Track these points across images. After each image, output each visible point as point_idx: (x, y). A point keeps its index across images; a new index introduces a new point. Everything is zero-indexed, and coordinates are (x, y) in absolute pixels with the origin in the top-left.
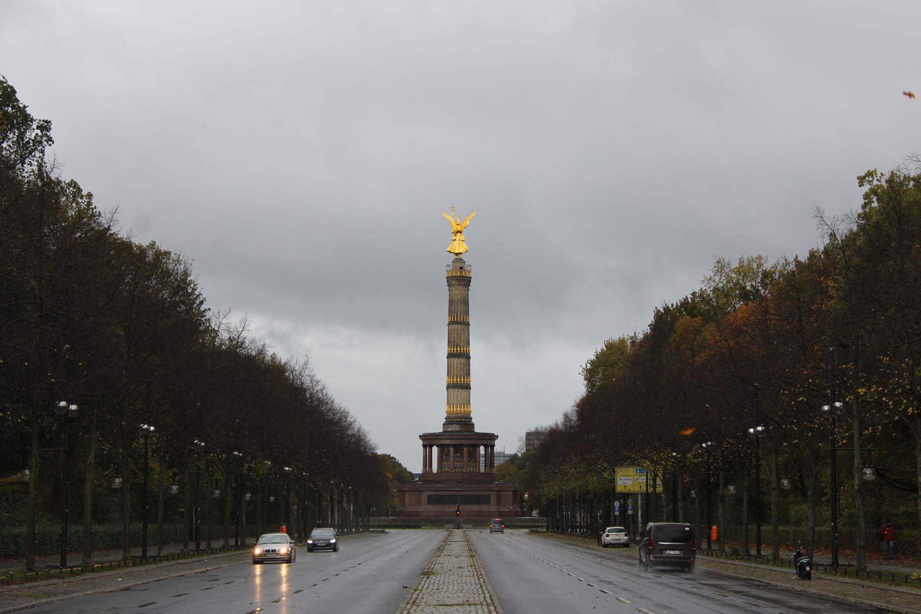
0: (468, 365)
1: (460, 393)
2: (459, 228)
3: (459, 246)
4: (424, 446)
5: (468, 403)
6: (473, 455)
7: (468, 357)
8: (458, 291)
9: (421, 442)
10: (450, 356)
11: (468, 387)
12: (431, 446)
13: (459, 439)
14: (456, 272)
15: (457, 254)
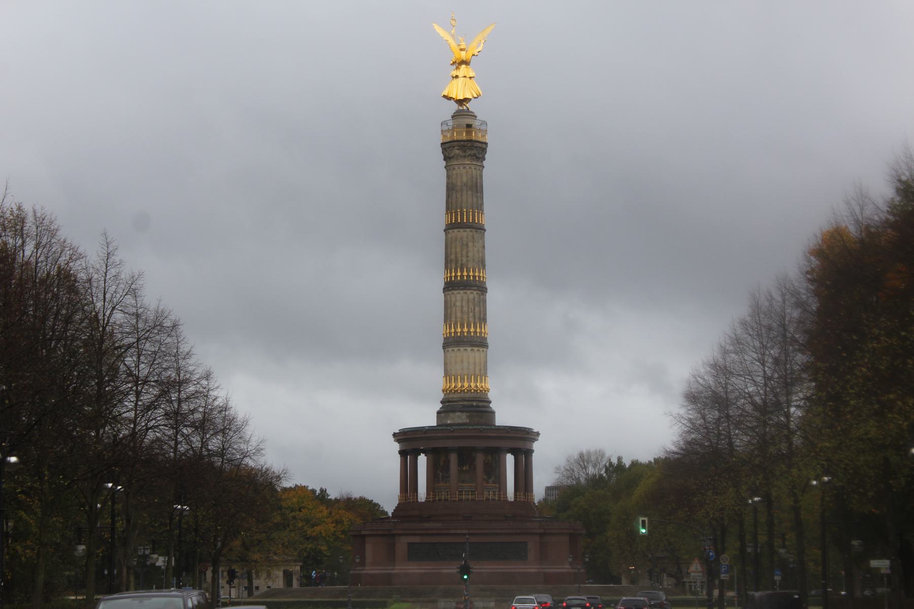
0: (482, 303)
1: (469, 355)
2: (463, 55)
3: (459, 90)
4: (403, 453)
5: (482, 372)
6: (495, 472)
7: (482, 289)
8: (464, 171)
9: (396, 447)
10: (450, 286)
11: (481, 343)
12: (416, 453)
13: (465, 444)
14: (459, 133)
15: (461, 102)
